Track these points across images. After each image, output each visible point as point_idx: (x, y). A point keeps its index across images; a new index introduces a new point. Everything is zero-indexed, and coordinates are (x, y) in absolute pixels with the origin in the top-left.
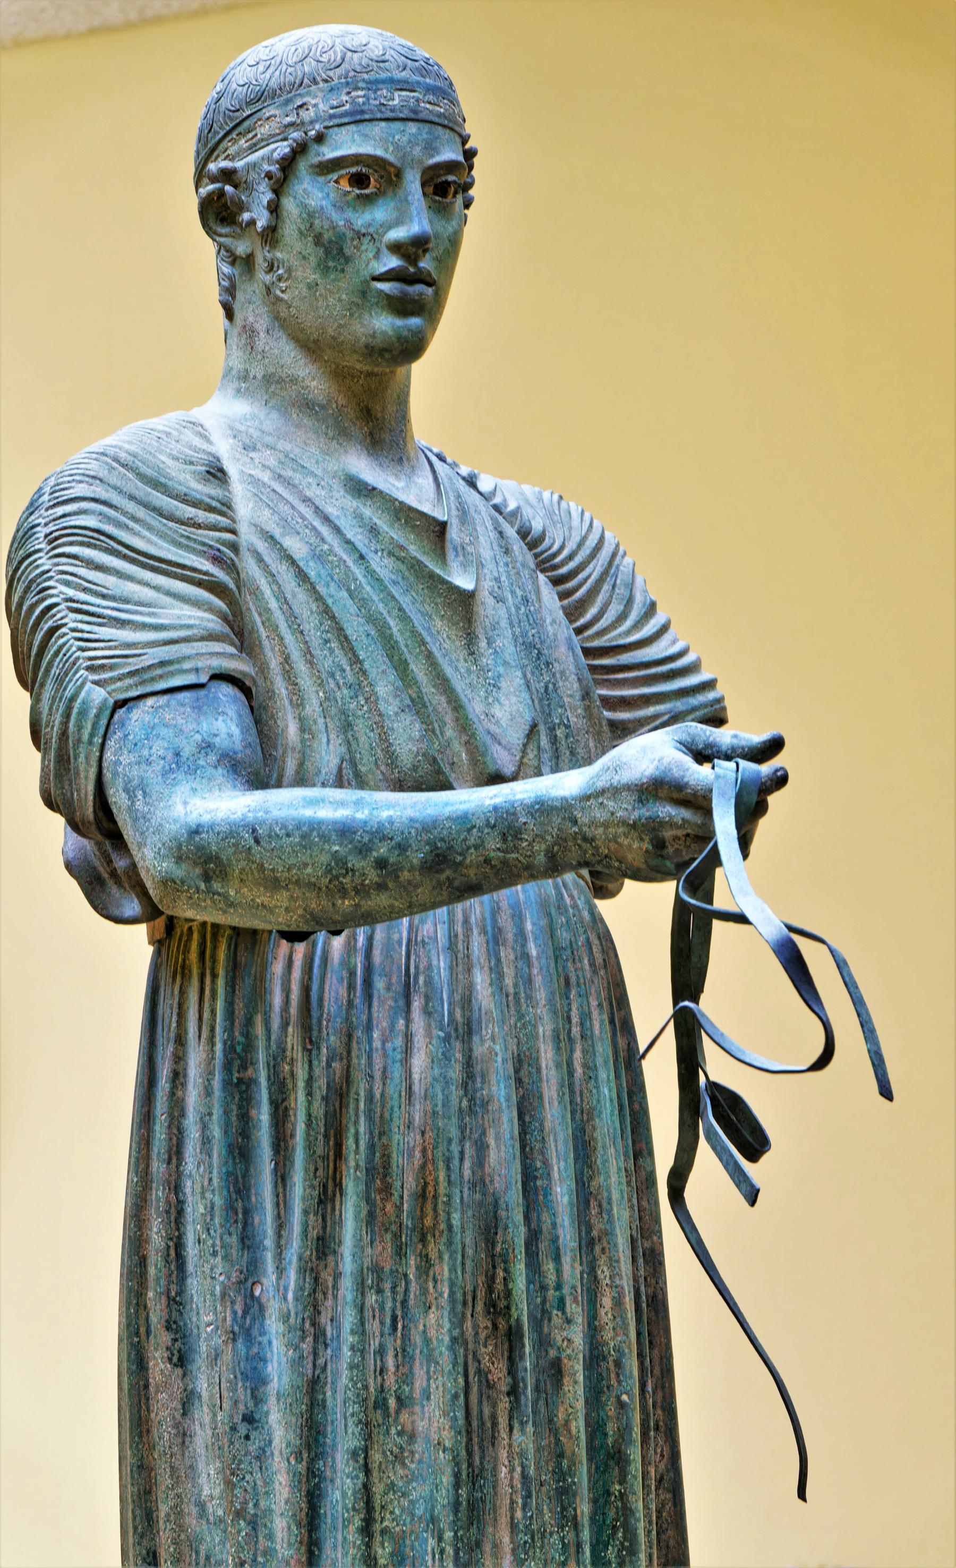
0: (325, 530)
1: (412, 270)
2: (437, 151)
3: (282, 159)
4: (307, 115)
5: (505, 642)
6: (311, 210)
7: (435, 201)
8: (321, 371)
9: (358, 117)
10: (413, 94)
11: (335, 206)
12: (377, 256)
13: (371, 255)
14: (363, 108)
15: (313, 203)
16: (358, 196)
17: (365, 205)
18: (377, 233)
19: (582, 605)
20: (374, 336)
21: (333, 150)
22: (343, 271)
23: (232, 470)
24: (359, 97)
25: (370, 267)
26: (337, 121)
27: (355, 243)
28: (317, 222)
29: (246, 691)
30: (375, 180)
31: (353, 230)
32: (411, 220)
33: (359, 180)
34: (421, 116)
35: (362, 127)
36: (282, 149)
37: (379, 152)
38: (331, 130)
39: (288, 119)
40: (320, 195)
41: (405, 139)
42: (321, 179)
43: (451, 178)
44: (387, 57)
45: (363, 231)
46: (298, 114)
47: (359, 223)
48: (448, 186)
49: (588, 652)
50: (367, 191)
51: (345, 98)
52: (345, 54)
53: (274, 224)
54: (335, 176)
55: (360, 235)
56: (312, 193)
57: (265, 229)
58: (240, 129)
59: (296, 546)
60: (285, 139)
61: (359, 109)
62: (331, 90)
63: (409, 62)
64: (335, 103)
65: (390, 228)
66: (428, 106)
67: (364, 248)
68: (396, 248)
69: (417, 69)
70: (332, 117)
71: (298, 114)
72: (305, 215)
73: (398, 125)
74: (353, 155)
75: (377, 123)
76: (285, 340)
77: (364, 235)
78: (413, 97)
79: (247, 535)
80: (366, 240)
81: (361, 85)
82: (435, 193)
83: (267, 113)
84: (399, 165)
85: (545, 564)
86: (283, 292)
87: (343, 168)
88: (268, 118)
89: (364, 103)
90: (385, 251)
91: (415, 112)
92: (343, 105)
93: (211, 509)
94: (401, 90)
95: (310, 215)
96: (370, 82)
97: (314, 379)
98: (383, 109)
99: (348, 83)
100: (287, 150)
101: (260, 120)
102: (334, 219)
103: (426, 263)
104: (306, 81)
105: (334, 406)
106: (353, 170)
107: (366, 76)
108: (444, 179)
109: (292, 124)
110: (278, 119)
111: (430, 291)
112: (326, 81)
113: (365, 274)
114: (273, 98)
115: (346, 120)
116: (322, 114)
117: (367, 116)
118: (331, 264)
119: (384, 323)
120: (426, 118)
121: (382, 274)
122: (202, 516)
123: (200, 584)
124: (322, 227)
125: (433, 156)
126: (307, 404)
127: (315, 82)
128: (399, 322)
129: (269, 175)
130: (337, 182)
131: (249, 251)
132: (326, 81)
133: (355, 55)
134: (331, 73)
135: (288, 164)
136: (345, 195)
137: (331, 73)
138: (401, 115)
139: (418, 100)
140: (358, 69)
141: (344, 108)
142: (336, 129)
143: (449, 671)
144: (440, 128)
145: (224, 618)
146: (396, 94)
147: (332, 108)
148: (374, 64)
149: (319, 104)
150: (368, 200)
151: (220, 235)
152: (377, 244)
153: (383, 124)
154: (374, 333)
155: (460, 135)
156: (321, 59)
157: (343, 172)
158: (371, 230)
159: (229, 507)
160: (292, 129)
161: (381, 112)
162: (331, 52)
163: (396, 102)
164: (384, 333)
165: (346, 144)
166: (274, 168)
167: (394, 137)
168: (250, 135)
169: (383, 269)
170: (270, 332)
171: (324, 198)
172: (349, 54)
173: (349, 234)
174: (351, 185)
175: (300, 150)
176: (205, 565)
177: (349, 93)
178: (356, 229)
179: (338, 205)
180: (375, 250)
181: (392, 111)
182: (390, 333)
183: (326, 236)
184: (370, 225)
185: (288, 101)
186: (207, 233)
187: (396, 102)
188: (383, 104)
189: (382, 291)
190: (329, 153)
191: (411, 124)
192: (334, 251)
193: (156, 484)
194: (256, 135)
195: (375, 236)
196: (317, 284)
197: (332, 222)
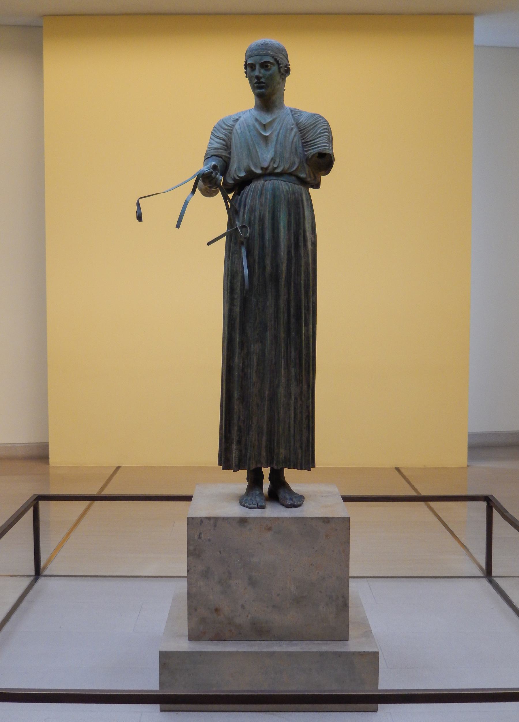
0: (246, 128)
2: (262, 60)
5: (274, 144)
19: (305, 135)
23: (241, 119)
29: (221, 158)
33: (252, 68)
49: (303, 143)
59: (239, 131)
79: (234, 131)
85: (299, 128)
93: (229, 126)
119: (259, 91)
122: (227, 127)
123: (222, 140)
143: (258, 150)
145: (223, 145)
159: (234, 126)
176: (223, 136)
193: (225, 123)
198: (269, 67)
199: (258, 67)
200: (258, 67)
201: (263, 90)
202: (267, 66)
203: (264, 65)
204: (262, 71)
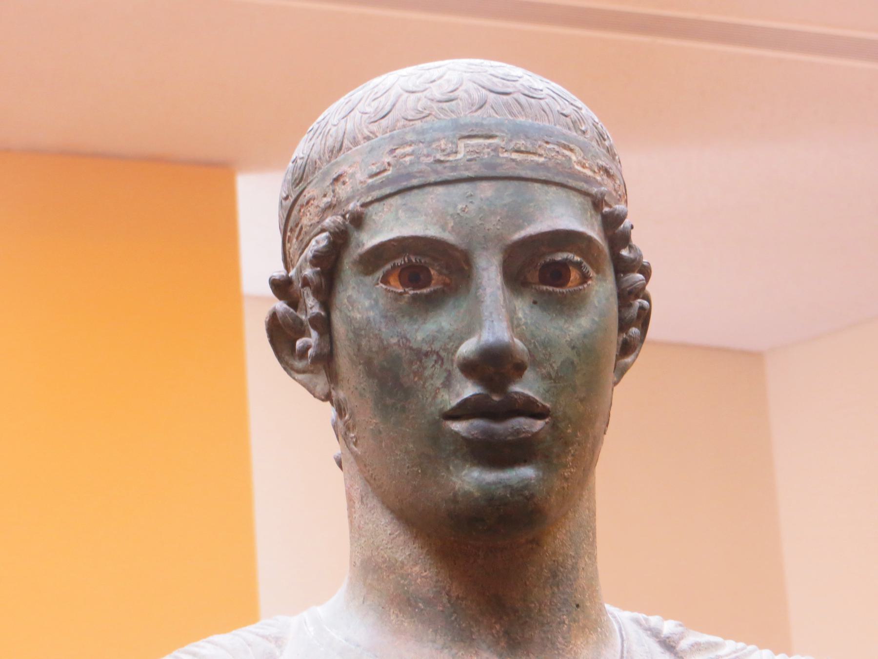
1: (496, 398)
3: (314, 257)
4: (343, 191)
6: (357, 326)
7: (543, 293)
8: (425, 552)
9: (404, 184)
10: (488, 142)
11: (386, 317)
12: (447, 384)
13: (438, 383)
14: (410, 170)
15: (358, 316)
16: (415, 298)
17: (427, 311)
18: (445, 350)
20: (454, 500)
21: (372, 237)
22: (403, 409)
24: (405, 155)
25: (439, 399)
26: (377, 194)
27: (415, 367)
28: (364, 342)
30: (440, 273)
31: (411, 348)
32: (481, 326)
33: (413, 276)
34: (500, 172)
35: (413, 198)
36: (320, 242)
37: (432, 232)
38: (370, 208)
39: (326, 200)
40: (367, 303)
41: (472, 207)
42: (369, 280)
43: (560, 256)
44: (460, 93)
45: (426, 348)
46: (334, 191)
47: (419, 338)
48: (582, 266)
50: (425, 291)
51: (388, 159)
52: (400, 96)
53: (326, 350)
54: (379, 274)
55: (420, 355)
56: (362, 301)
57: (317, 359)
58: (291, 224)
60: (323, 230)
61: (403, 171)
62: (372, 150)
63: (492, 96)
64: (375, 169)
65: (461, 341)
66: (515, 156)
67: (427, 373)
68: (470, 368)
69: (507, 105)
70: (371, 188)
71: (334, 191)
72: (351, 335)
73: (464, 188)
74: (390, 241)
75: (430, 189)
76: (379, 510)
77: (427, 354)
78: (488, 146)
80: (430, 362)
81: (410, 137)
82: (543, 281)
83: (307, 194)
84: (463, 247)
86: (355, 444)
87: (387, 261)
88: (308, 203)
89: (412, 163)
90: (458, 374)
91: (493, 166)
92: (385, 170)
94: (470, 137)
95: (358, 332)
96: (423, 132)
97: (416, 564)
98: (439, 167)
99: (392, 138)
100: (324, 243)
101: (302, 206)
102: (383, 336)
103: (527, 387)
104: (346, 143)
105: (445, 600)
106: (399, 262)
107: (418, 124)
108: (548, 259)
109: (330, 207)
110: (316, 202)
111: (539, 424)
112: (368, 138)
113: (433, 411)
114: (314, 173)
115: (387, 190)
116: (359, 187)
117: (415, 182)
118: (389, 401)
119: (473, 478)
120: (511, 173)
121: (454, 409)
124: (370, 350)
125: (520, 227)
126: (408, 599)
127: (355, 143)
128: (491, 476)
129: (306, 282)
130: (385, 280)
131: (326, 390)
132: (368, 138)
133: (413, 96)
134: (374, 127)
135: (329, 263)
136: (396, 300)
137: (374, 127)
138: (467, 174)
139: (495, 149)
140: (411, 115)
141: (385, 174)
142: (376, 205)
144: (537, 186)
146: (461, 144)
147: (372, 176)
148: (435, 106)
149: (357, 173)
150: (430, 303)
151: (299, 372)
152: (447, 366)
153: (440, 190)
154: (455, 495)
155: (586, 194)
156: (368, 110)
157: (388, 267)
158: (436, 346)
160: (329, 212)
161: (436, 172)
162: (383, 99)
163: (459, 156)
164: (468, 494)
165: (388, 226)
166: (308, 272)
167: (456, 206)
168: (298, 229)
169: (454, 402)
170: (364, 499)
171: (372, 307)
172: (406, 95)
173: (405, 355)
174: (404, 285)
175: (340, 240)
177: (393, 151)
178: (415, 346)
179: (389, 314)
180: (445, 374)
181: (454, 169)
182: (477, 494)
183: (375, 362)
184: (434, 339)
185: (326, 174)
186: (285, 369)
187: (459, 156)
188: (440, 162)
189: (457, 433)
190: (369, 240)
191: (485, 184)
192: (392, 380)
194: (302, 228)
195: (443, 354)
196: (380, 432)
197: (382, 341)
198: (574, 275)
199: (489, 275)
200: (489, 275)
201: (527, 472)
202: (557, 274)
203: (541, 268)
204: (523, 308)
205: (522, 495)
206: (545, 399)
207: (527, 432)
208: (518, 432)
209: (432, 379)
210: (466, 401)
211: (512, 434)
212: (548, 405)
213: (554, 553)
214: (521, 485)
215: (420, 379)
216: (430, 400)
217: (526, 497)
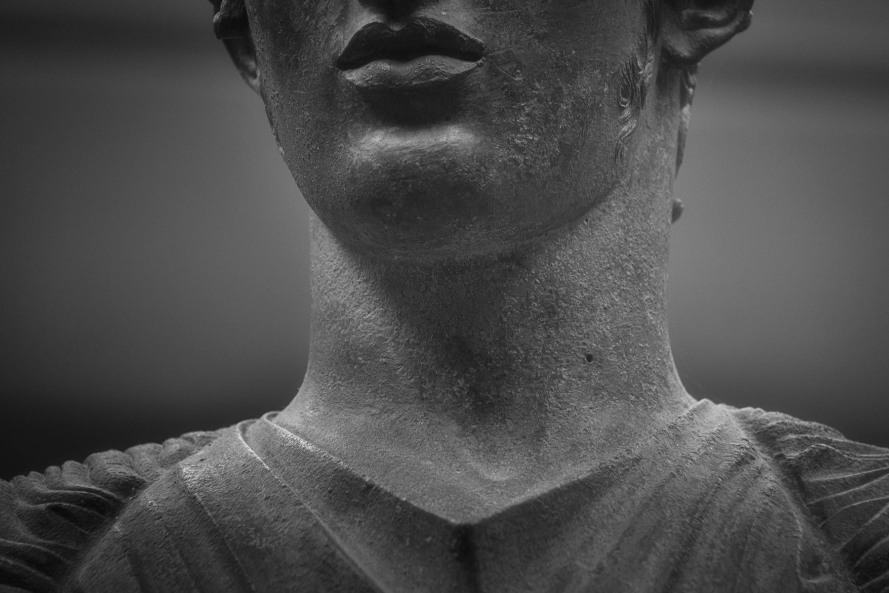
1: (396, 28)
12: (343, 20)
13: (333, 19)
23: (148, 498)
113: (325, 58)
164: (366, 166)
189: (351, 83)
205: (438, 163)
206: (474, 32)
207: (442, 73)
208: (428, 73)
209: (326, 15)
210: (359, 36)
211: (419, 77)
212: (480, 40)
213: (551, 281)
214: (436, 149)
215: (312, 18)
216: (323, 44)
217: (444, 166)
